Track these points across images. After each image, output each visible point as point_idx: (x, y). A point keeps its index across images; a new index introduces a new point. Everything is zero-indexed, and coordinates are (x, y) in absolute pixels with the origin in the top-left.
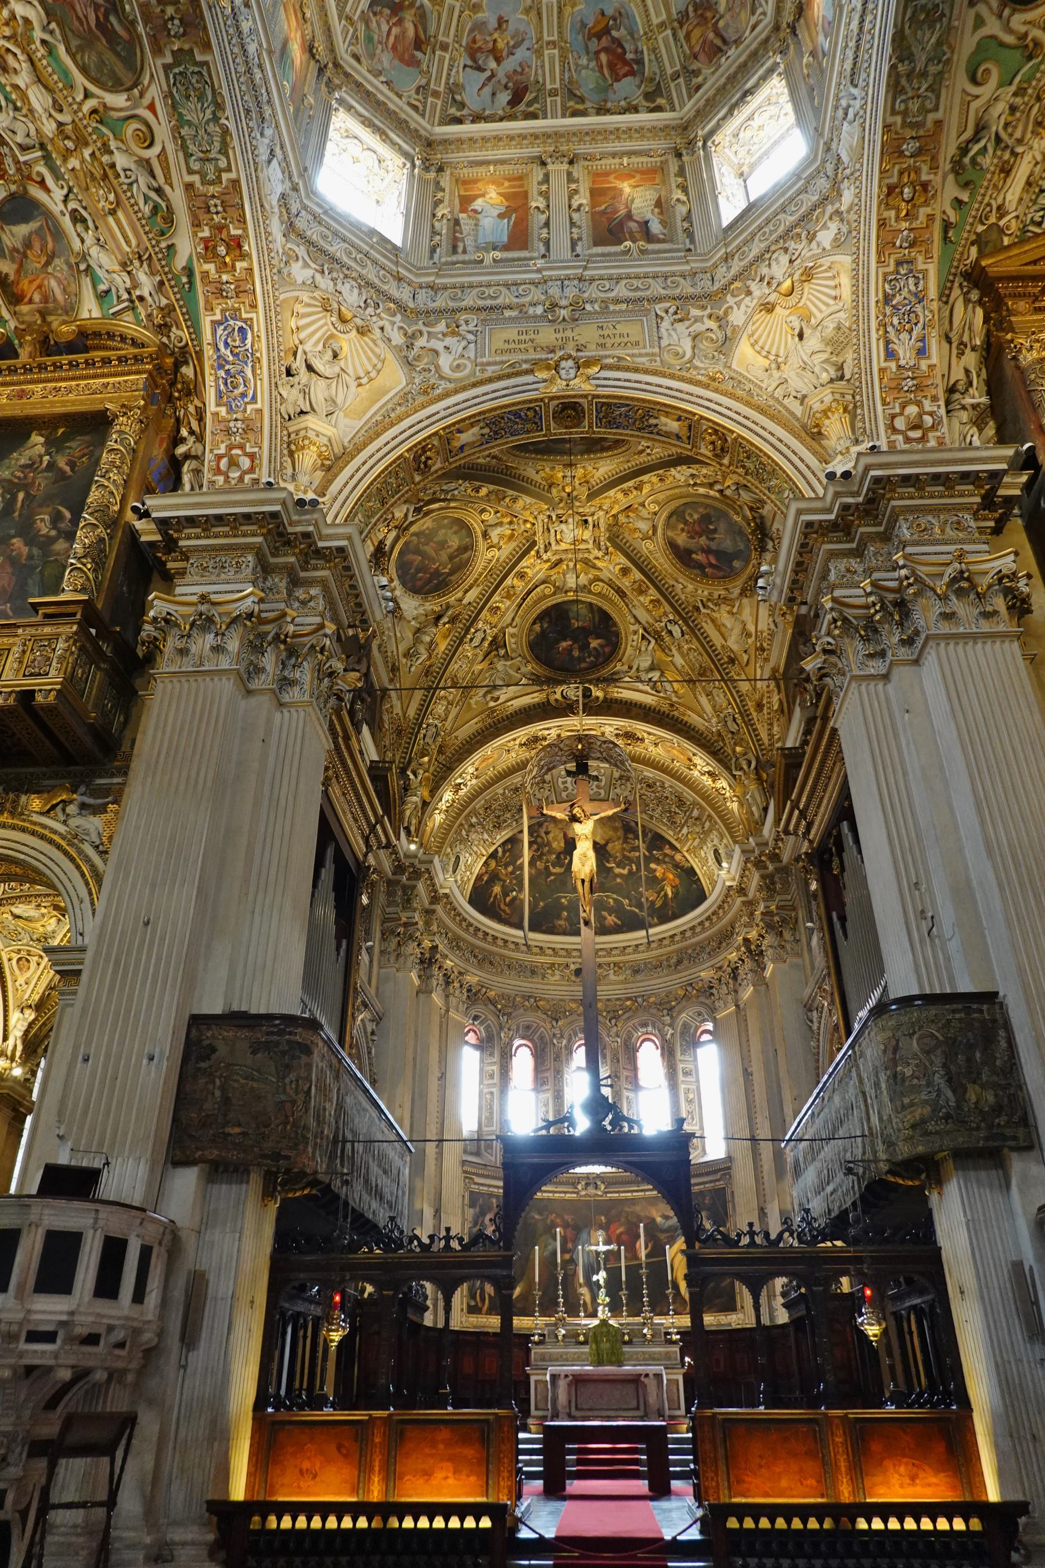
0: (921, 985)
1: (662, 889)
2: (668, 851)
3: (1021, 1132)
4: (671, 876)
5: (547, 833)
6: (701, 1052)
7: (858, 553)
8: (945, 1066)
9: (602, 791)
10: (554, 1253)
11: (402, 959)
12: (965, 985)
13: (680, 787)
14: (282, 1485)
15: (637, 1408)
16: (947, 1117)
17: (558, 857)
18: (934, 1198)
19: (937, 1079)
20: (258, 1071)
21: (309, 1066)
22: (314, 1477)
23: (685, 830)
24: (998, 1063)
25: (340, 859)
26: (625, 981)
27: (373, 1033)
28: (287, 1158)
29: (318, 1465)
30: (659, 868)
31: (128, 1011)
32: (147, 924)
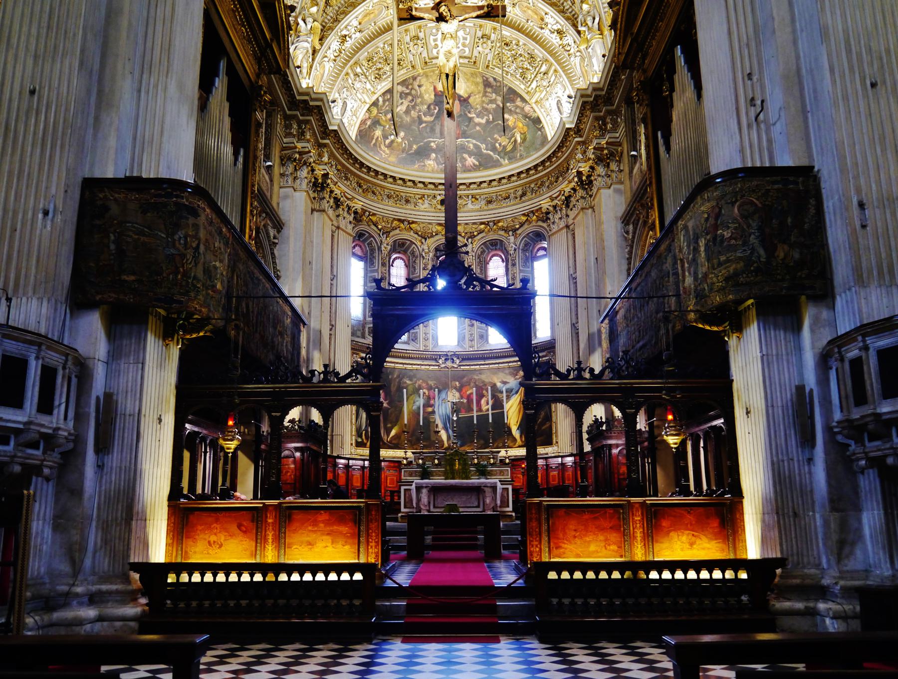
0: (743, 160)
1: (513, 135)
2: (519, 102)
4: (521, 125)
5: (420, 86)
6: (536, 264)
8: (760, 229)
9: (467, 49)
10: (419, 408)
11: (298, 181)
12: (785, 160)
13: (532, 45)
14: (195, 552)
15: (478, 506)
17: (429, 107)
18: (732, 341)
20: (149, 228)
21: (196, 227)
22: (221, 546)
23: (534, 85)
24: (806, 226)
25: (232, 72)
26: (481, 210)
27: (275, 238)
28: (180, 302)
29: (223, 538)
30: (511, 118)
31: (21, 171)
32: (32, 92)
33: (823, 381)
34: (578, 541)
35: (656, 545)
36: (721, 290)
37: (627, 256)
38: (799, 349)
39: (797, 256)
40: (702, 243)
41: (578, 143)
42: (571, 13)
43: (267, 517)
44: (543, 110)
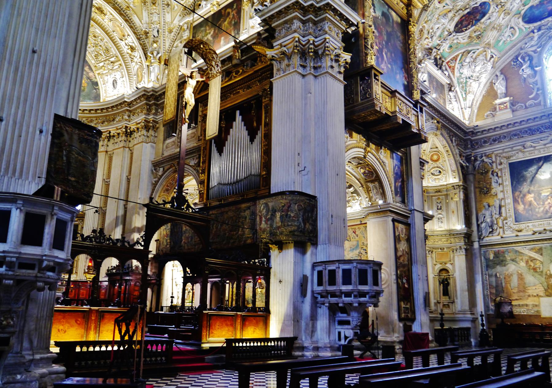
3: (315, 239)
7: (304, 22)
8: (303, 216)
13: (110, 45)
16: (301, 231)
19: (301, 219)
20: (83, 152)
22: (65, 332)
23: (102, 64)
29: (67, 327)
31: (26, 100)
32: (34, 52)
33: (312, 275)
34: (219, 330)
35: (244, 332)
36: (286, 235)
37: (154, 182)
38: (303, 261)
39: (311, 228)
40: (278, 215)
41: (127, 110)
42: (143, 42)
43: (91, 316)
44: (101, 80)
